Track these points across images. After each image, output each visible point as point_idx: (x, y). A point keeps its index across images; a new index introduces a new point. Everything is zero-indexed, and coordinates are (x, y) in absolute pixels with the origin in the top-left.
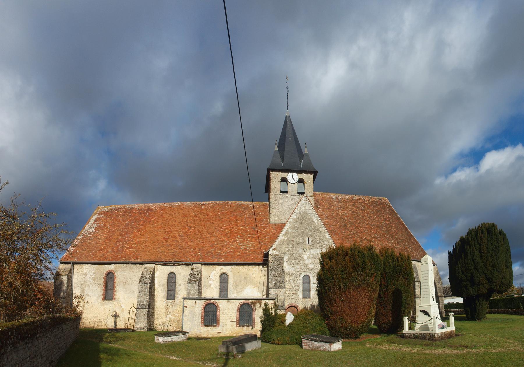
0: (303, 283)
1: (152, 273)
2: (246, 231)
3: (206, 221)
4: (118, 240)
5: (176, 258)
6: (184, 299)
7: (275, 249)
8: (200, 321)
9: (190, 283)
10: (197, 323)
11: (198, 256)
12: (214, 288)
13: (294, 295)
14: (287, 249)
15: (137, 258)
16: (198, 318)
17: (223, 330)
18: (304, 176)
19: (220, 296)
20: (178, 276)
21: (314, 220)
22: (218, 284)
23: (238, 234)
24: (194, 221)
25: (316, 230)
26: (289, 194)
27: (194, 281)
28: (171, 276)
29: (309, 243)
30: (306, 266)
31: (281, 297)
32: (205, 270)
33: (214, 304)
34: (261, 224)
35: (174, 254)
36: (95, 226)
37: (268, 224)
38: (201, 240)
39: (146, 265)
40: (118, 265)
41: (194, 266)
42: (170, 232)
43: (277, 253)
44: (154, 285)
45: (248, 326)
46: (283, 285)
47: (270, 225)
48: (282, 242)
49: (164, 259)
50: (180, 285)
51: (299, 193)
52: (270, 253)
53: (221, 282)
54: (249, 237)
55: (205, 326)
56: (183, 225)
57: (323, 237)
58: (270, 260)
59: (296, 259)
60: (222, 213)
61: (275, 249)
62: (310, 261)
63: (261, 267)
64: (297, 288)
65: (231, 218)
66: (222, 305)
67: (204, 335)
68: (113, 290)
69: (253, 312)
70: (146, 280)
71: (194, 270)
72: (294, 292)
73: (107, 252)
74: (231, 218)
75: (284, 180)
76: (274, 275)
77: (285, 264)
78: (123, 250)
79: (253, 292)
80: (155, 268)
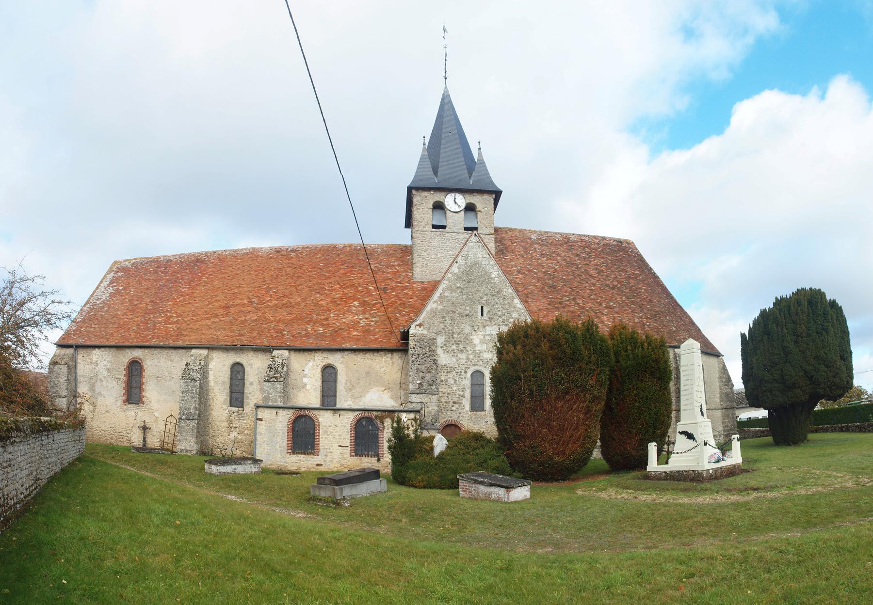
0: (472, 385)
1: (202, 363)
2: (369, 293)
3: (298, 278)
5: (244, 339)
6: (258, 407)
7: (420, 325)
8: (285, 444)
9: (268, 381)
10: (280, 447)
11: (283, 337)
12: (312, 390)
13: (456, 406)
14: (442, 326)
15: (178, 340)
16: (282, 439)
17: (325, 461)
18: (477, 200)
19: (323, 404)
20: (248, 369)
21: (493, 276)
23: (355, 298)
24: (277, 278)
25: (497, 293)
26: (447, 230)
27: (276, 378)
28: (236, 368)
29: (482, 315)
30: (478, 355)
31: (430, 408)
32: (297, 362)
33: (311, 419)
34: (397, 283)
35: (242, 332)
37: (410, 282)
38: (288, 310)
39: (193, 351)
40: (147, 351)
41: (275, 353)
42: (235, 296)
43: (425, 332)
45: (372, 456)
46: (434, 387)
47: (414, 283)
48: (434, 312)
50: (251, 384)
51: (466, 229)
52: (411, 331)
53: (323, 382)
54: (375, 304)
55: (294, 453)
56: (257, 284)
57: (510, 305)
58: (411, 343)
59: (461, 343)
60: (326, 264)
61: (420, 325)
62: (484, 347)
63: (396, 356)
64: (462, 393)
65: (342, 271)
66: (325, 419)
67: (293, 468)
69: (380, 433)
71: (276, 359)
72: (455, 400)
73: (129, 329)
74: (342, 271)
75: (439, 207)
76: (418, 369)
77: (440, 351)
78: (155, 326)
79: (379, 398)
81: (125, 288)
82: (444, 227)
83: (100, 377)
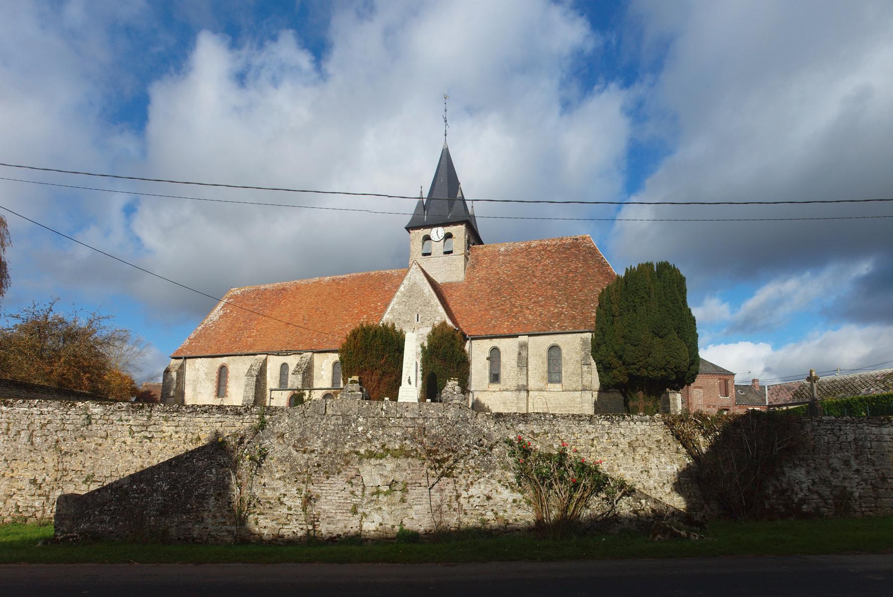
4: (240, 329)
44: (265, 378)
49: (277, 348)
68: (225, 386)
70: (253, 372)
80: (266, 359)
83: (201, 379)
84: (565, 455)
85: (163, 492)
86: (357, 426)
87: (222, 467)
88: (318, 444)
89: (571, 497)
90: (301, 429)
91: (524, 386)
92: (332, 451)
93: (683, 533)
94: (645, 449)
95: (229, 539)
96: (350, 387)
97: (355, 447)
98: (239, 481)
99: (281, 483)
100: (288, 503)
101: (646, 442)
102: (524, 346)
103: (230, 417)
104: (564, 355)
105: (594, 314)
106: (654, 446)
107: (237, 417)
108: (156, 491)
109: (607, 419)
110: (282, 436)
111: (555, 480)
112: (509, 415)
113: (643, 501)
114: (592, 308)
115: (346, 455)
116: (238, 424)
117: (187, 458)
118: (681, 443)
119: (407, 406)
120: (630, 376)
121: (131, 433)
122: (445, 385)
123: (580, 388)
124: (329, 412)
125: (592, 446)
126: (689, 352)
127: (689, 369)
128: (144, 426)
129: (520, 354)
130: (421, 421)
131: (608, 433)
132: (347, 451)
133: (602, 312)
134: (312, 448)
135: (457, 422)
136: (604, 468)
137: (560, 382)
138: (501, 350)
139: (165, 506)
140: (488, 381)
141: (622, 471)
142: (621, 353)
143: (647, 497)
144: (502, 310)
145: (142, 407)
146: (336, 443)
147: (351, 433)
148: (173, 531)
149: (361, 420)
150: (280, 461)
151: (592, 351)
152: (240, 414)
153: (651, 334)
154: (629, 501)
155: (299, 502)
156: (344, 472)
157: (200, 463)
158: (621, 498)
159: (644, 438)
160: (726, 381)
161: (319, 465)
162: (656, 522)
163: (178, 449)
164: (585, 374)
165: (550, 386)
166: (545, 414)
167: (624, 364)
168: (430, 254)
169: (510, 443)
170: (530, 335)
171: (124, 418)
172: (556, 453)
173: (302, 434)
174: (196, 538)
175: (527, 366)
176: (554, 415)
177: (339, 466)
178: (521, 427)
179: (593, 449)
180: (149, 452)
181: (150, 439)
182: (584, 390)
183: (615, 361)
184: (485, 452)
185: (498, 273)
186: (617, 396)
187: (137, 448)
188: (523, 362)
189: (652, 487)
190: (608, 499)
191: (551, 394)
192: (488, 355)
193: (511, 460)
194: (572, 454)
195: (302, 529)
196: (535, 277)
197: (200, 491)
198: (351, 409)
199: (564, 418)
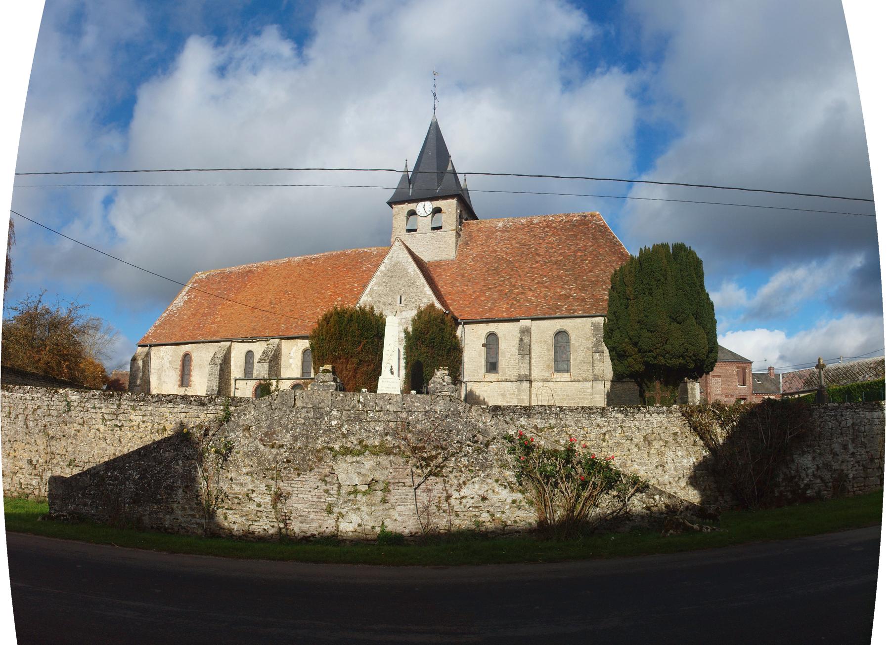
4: (204, 315)
15: (214, 336)
22: (300, 363)
36: (186, 298)
44: (229, 367)
68: (189, 375)
75: (412, 213)
80: (230, 346)
81: (195, 297)
82: (415, 230)
83: (165, 368)
84: (573, 451)
85: (134, 481)
86: (330, 420)
87: (188, 459)
88: (287, 439)
89: (579, 496)
90: (268, 422)
91: (526, 376)
92: (303, 446)
93: (696, 526)
94: (661, 443)
95: (200, 531)
96: (322, 377)
97: (328, 443)
98: (206, 474)
99: (248, 479)
100: (257, 500)
101: (662, 435)
102: (526, 331)
103: (195, 407)
104: (572, 341)
105: (606, 297)
106: (670, 439)
107: (201, 408)
108: (128, 479)
109: (621, 412)
110: (248, 428)
111: (562, 479)
112: (508, 408)
113: (657, 497)
114: (604, 290)
115: (319, 451)
116: (202, 415)
117: (154, 448)
118: (699, 435)
119: (389, 398)
120: (646, 364)
121: (104, 420)
122: (432, 374)
123: (591, 377)
124: (299, 404)
125: (604, 440)
126: (708, 339)
127: (708, 357)
128: (114, 414)
129: (521, 340)
130: (404, 415)
131: (621, 427)
132: (319, 446)
133: (615, 294)
134: (281, 443)
135: (446, 417)
136: (616, 464)
137: (568, 371)
138: (500, 335)
139: (137, 495)
140: (483, 370)
141: (636, 467)
142: (636, 340)
143: (661, 493)
144: (501, 291)
145: (112, 396)
146: (307, 438)
147: (323, 427)
148: (146, 519)
149: (334, 413)
150: (247, 455)
151: (604, 337)
152: (204, 405)
153: (668, 320)
154: (642, 498)
155: (268, 499)
156: (316, 470)
157: (167, 454)
158: (633, 494)
159: (660, 431)
160: (744, 369)
161: (288, 461)
162: (670, 518)
163: (146, 439)
164: (597, 363)
165: (557, 376)
166: (550, 407)
167: (639, 351)
168: (415, 230)
169: (510, 439)
170: (533, 319)
171: (98, 406)
172: (563, 449)
173: (269, 427)
174: (168, 528)
175: (530, 353)
176: (561, 408)
177: (311, 463)
178: (523, 421)
179: (605, 444)
180: (120, 440)
181: (121, 427)
182: (595, 379)
183: (630, 349)
184: (480, 449)
185: (495, 251)
186: (632, 386)
187: (109, 436)
188: (525, 349)
189: (666, 482)
190: (619, 497)
191: (557, 385)
192: (483, 341)
193: (510, 458)
194: (581, 450)
195: (273, 527)
196: (539, 255)
197: (168, 482)
198: (323, 401)
199: (572, 411)
